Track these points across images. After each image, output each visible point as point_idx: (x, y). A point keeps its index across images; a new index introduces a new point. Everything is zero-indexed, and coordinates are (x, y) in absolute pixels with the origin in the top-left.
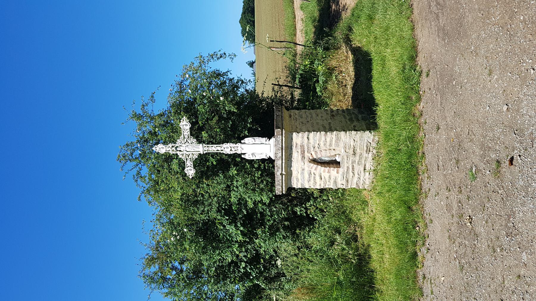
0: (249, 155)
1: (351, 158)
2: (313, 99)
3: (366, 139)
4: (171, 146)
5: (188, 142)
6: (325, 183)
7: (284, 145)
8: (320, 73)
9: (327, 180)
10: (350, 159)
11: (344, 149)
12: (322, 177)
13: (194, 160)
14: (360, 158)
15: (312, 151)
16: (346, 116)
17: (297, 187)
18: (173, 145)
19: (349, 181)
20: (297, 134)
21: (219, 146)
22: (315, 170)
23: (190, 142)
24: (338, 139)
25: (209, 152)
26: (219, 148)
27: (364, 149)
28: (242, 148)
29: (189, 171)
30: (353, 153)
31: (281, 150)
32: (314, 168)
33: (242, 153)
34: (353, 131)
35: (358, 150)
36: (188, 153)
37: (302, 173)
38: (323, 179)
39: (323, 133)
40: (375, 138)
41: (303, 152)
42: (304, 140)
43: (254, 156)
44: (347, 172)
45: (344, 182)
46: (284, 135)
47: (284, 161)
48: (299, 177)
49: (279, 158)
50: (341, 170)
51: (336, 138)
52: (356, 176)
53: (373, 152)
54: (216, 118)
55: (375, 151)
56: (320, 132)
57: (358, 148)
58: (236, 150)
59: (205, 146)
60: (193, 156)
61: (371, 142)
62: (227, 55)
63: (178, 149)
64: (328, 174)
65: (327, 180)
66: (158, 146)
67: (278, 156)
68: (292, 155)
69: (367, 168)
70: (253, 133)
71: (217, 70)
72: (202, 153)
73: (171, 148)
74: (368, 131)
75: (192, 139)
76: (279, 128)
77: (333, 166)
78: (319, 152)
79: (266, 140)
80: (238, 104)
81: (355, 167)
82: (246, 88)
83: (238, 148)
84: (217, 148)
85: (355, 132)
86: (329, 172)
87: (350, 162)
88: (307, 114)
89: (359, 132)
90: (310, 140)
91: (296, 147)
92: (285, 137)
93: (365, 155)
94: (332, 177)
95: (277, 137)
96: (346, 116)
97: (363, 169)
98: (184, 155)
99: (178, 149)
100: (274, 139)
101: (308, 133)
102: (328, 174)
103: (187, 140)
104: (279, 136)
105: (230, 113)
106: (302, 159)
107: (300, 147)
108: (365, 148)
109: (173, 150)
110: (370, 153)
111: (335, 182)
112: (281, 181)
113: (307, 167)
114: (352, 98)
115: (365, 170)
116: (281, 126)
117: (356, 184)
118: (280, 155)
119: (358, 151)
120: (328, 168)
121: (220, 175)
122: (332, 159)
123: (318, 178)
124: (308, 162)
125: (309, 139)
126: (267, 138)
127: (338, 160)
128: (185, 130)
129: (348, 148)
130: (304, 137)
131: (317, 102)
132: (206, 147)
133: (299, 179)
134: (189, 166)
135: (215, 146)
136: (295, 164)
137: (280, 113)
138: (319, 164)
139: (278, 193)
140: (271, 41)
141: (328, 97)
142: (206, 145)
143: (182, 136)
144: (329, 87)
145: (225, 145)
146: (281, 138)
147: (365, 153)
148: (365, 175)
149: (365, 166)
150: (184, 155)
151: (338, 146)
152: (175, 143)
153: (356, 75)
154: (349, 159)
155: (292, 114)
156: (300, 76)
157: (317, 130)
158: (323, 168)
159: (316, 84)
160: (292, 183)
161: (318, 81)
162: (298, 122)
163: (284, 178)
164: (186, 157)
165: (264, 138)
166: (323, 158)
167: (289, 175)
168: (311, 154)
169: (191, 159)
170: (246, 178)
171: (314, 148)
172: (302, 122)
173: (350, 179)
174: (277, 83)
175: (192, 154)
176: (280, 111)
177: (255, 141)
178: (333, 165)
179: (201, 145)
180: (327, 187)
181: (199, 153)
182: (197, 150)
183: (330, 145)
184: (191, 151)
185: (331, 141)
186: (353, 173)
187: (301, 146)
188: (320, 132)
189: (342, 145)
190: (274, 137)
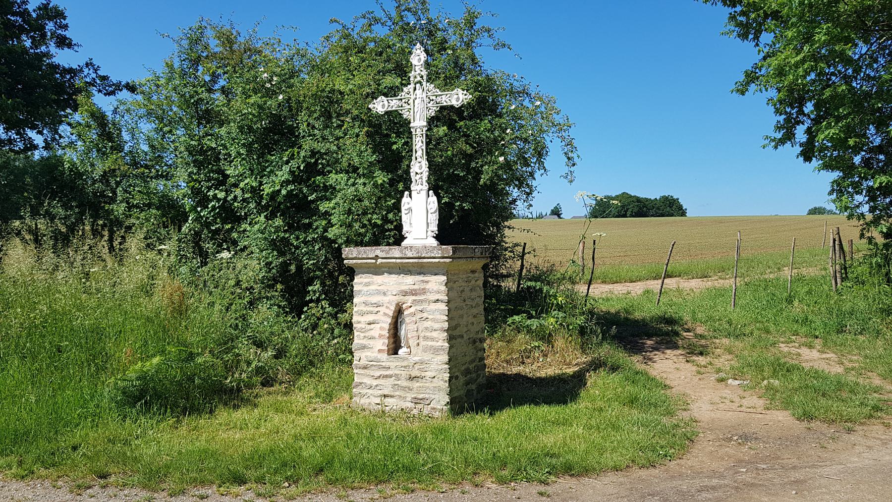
0: (408, 203)
1: (404, 374)
2: (502, 310)
3: (436, 396)
4: (422, 73)
5: (429, 103)
6: (362, 330)
7: (425, 260)
8: (543, 321)
9: (367, 334)
10: (402, 372)
11: (420, 360)
12: (372, 326)
13: (400, 112)
14: (404, 388)
15: (415, 308)
16: (474, 364)
17: (356, 284)
18: (425, 78)
19: (366, 371)
20: (444, 283)
21: (423, 154)
23: (429, 105)
24: (436, 351)
25: (414, 136)
26: (419, 153)
29: (382, 103)
30: (413, 375)
31: (417, 256)
32: (387, 311)
33: (413, 192)
34: (448, 375)
35: (418, 384)
36: (411, 101)
37: (378, 292)
39: (446, 325)
40: (437, 412)
41: (413, 293)
43: (407, 212)
44: (381, 367)
45: (363, 362)
46: (442, 260)
47: (398, 261)
48: (372, 287)
49: (404, 252)
50: (384, 356)
52: (375, 383)
53: (415, 410)
54: (470, 150)
55: (415, 412)
56: (447, 321)
57: (421, 385)
59: (422, 131)
61: (431, 405)
62: (572, 169)
64: (377, 336)
66: (423, 52)
67: (407, 252)
69: (388, 400)
70: (445, 211)
71: (547, 152)
72: (411, 125)
73: (419, 74)
74: (449, 401)
75: (435, 108)
76: (454, 252)
77: (391, 343)
78: (414, 319)
80: (492, 187)
81: (389, 379)
82: (518, 201)
83: (420, 185)
84: (420, 149)
85: (447, 379)
86: (381, 336)
88: (478, 299)
89: (447, 385)
91: (423, 281)
92: (439, 262)
93: (410, 396)
94: (371, 342)
95: (439, 250)
96: (474, 364)
97: (385, 394)
98: (409, 96)
99: (418, 86)
100: (436, 245)
101: (446, 301)
102: (377, 336)
103: (433, 100)
104: (440, 252)
105: (478, 173)
106: (402, 291)
108: (421, 396)
109: (415, 77)
110: (413, 405)
111: (364, 347)
112: (364, 256)
114: (503, 374)
115: (385, 396)
116: (458, 256)
117: (361, 381)
118: (410, 254)
119: (416, 385)
120: (388, 335)
121: (374, 156)
122: (403, 341)
123: (371, 318)
124: (396, 302)
125: (435, 302)
126: (437, 232)
127: (400, 352)
131: (497, 317)
133: (369, 287)
134: (389, 103)
137: (478, 254)
138: (394, 320)
139: (345, 251)
140: (594, 241)
141: (503, 335)
142: (424, 132)
143: (440, 93)
144: (521, 336)
145: (425, 163)
146: (437, 255)
147: (413, 396)
148: (375, 396)
149: (392, 397)
150: (409, 96)
151: (425, 351)
152: (427, 81)
153: (540, 378)
154: (403, 369)
155: (476, 275)
156: (538, 288)
157: (450, 316)
158: (387, 326)
159: (525, 315)
160: (363, 276)
161: (530, 317)
162: (463, 284)
164: (404, 99)
165: (437, 229)
166: (404, 327)
167: (376, 270)
168: (411, 307)
169: (402, 107)
170: (370, 199)
171: (421, 311)
172: (463, 291)
173: (368, 371)
174: (526, 251)
175: (410, 109)
176: (482, 254)
178: (393, 343)
179: (425, 124)
180: (356, 334)
181: (412, 121)
182: (417, 117)
183: (426, 338)
185: (433, 339)
186: (380, 377)
187: (424, 289)
188: (447, 321)
189: (427, 357)
190: (438, 245)
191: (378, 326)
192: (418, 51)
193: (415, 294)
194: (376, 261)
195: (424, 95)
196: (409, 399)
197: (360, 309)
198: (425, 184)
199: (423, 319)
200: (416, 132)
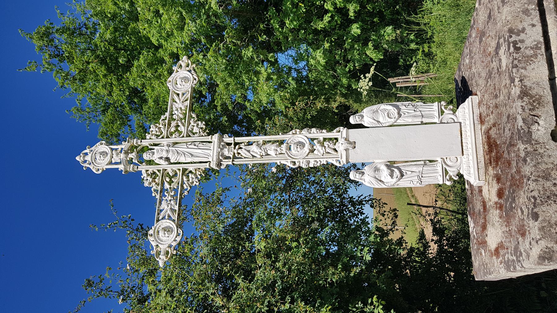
25: (237, 162)
31: (536, 14)
33: (352, 161)
36: (170, 169)
49: (530, 52)
59: (229, 144)
60: (184, 177)
63: (146, 156)
66: (93, 148)
67: (529, 42)
73: (127, 153)
79: (443, 112)
84: (264, 147)
128: (178, 95)
132: (233, 146)
135: (261, 142)
175: (184, 170)
177: (400, 115)
179: (215, 138)
184: (182, 159)
192: (88, 158)
195: (165, 142)
198: (334, 134)
200: (228, 158)
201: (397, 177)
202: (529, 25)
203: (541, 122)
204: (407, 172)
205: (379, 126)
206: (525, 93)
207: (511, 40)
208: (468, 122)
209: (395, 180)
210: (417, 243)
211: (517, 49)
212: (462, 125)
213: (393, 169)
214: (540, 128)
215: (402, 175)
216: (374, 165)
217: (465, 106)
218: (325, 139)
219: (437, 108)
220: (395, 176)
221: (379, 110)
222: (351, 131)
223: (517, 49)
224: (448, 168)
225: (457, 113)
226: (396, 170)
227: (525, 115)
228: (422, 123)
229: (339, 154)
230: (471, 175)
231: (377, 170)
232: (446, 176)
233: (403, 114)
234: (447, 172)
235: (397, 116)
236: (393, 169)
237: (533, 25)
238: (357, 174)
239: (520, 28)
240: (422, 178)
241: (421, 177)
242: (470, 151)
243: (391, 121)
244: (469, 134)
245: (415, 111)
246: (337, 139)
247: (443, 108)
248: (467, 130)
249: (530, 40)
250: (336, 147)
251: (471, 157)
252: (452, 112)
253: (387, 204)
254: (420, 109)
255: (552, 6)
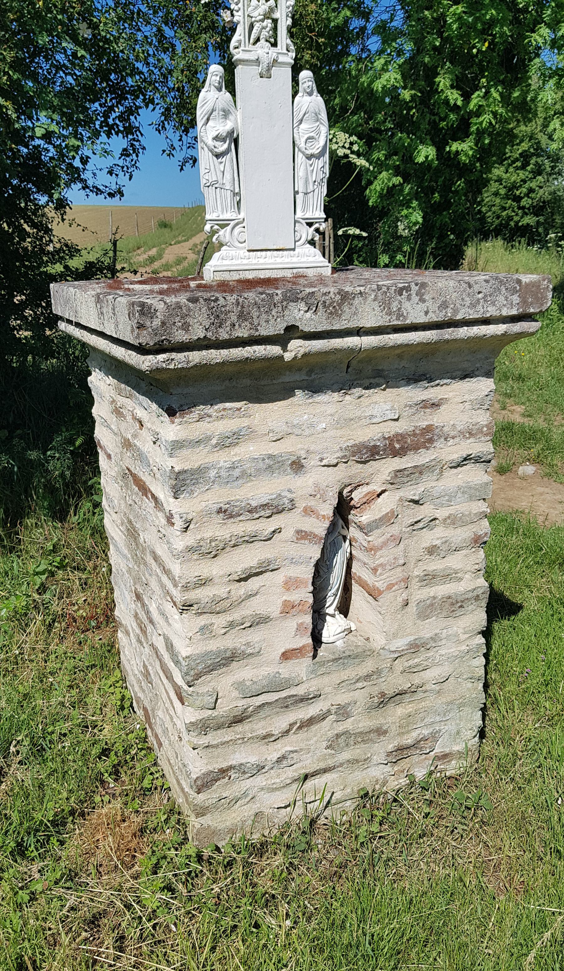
7: (464, 332)
9: (236, 615)
12: (254, 583)
19: (239, 728)
22: (298, 532)
27: (405, 737)
28: (269, 69)
30: (390, 692)
33: (239, 71)
38: (242, 592)
42: (457, 440)
49: (394, 306)
51: (459, 599)
58: (252, 27)
64: (274, 610)
65: (236, 615)
67: (407, 305)
68: (378, 385)
69: (309, 784)
78: (395, 530)
79: (310, 225)
81: (314, 728)
87: (342, 698)
90: (454, 471)
92: (505, 334)
95: (514, 291)
102: (274, 610)
104: (516, 299)
107: (424, 424)
108: (409, 740)
110: (388, 768)
112: (242, 332)
113: (316, 485)
115: (306, 777)
117: (224, 765)
129: (411, 663)
130: (472, 440)
133: (237, 450)
136: (331, 409)
147: (390, 747)
149: (325, 771)
154: (360, 685)
160: (212, 410)
163: (260, 351)
171: (416, 502)
177: (309, 157)
187: (429, 429)
191: (279, 577)
193: (396, 453)
194: (285, 349)
196: (380, 757)
197: (208, 534)
199: (421, 525)
201: (215, 147)
202: (428, 307)
203: (308, 315)
204: (223, 164)
205: (295, 122)
206: (345, 297)
207: (413, 285)
208: (295, 260)
209: (210, 143)
210: (59, 240)
211: (400, 292)
212: (292, 252)
213: (228, 142)
214: (302, 312)
215: (218, 156)
216: (232, 109)
217: (317, 257)
218: (275, 21)
219: (317, 216)
220: (218, 144)
221: (318, 123)
222: (288, 71)
223: (400, 292)
224: (229, 228)
225: (308, 245)
226: (226, 146)
227: (318, 295)
228: (296, 193)
229: (251, 47)
230: (220, 261)
231: (226, 114)
232: (217, 224)
233: (311, 162)
234: (223, 226)
235: (309, 152)
236: (228, 142)
237: (426, 313)
238: (218, 78)
239: (426, 297)
240: (214, 188)
241: (216, 186)
242: (254, 261)
243: (301, 143)
244: (279, 260)
245: (315, 182)
246: (274, 45)
247: (317, 225)
248: (283, 258)
249: (409, 308)
250: (262, 41)
251: (245, 261)
252: (310, 238)
253: (130, 179)
254: (316, 191)
255: (447, 337)
